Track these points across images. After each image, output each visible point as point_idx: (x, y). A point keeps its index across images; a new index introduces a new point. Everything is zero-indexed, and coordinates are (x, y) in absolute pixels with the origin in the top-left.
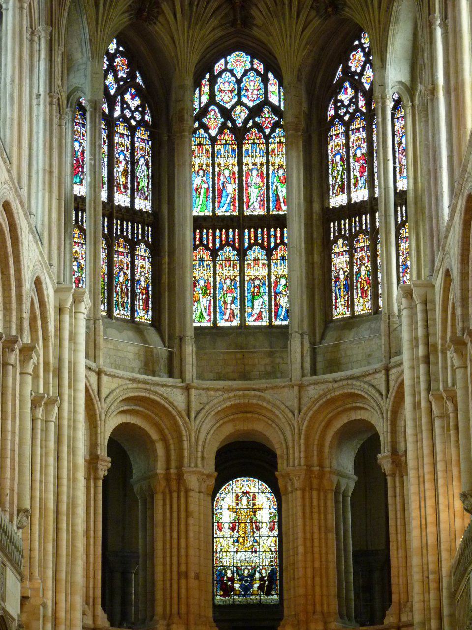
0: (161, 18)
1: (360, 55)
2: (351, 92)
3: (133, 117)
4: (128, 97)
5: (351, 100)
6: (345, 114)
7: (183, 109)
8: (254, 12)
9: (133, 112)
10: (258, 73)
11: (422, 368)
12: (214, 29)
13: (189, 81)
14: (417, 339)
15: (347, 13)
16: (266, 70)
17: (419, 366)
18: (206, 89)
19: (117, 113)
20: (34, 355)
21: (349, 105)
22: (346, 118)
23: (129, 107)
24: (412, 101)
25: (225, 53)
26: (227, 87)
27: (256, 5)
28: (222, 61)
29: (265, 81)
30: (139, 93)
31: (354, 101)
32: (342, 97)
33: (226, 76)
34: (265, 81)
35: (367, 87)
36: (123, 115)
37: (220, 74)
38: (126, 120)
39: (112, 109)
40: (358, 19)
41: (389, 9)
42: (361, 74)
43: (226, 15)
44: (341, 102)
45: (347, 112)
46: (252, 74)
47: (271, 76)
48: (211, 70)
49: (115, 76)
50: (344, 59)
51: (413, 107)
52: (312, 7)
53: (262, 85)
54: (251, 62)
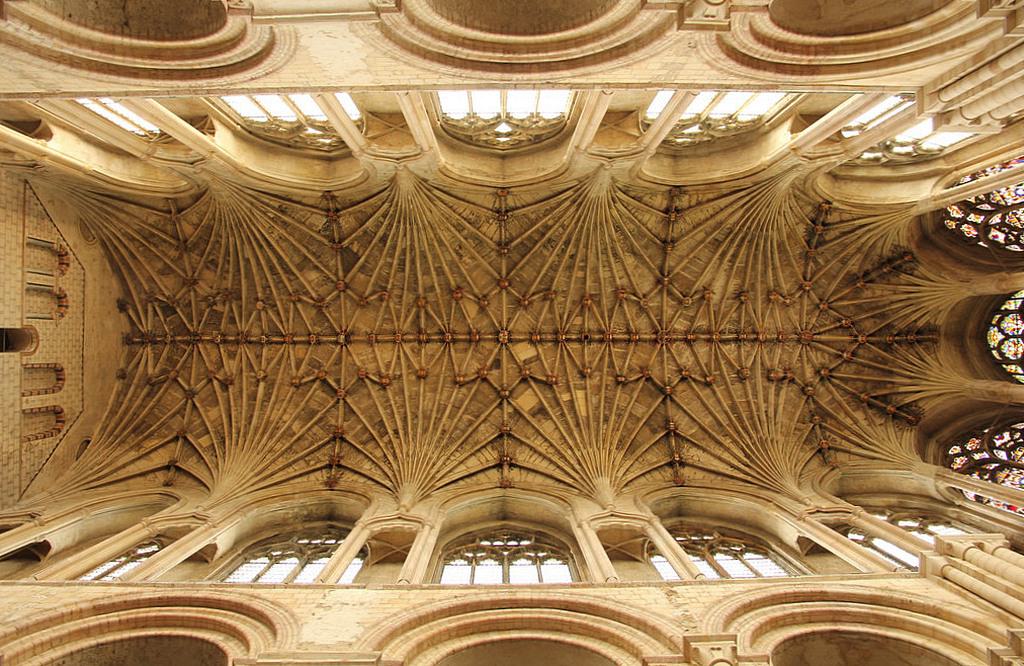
0: (920, 404)
1: (964, 227)
2: (994, 232)
3: (1015, 441)
4: (998, 443)
5: (999, 230)
6: (1013, 235)
7: (988, 392)
8: (920, 324)
9: (1012, 440)
10: (1001, 319)
11: (1005, 65)
12: (937, 360)
13: (997, 386)
14: (984, 85)
15: (904, 243)
16: (997, 310)
17: (1012, 70)
18: (1013, 367)
19: (1002, 455)
20: (694, 645)
21: (1003, 232)
22: (1016, 233)
23: (1005, 444)
24: (950, 172)
25: (989, 350)
26: (1013, 349)
27: (915, 321)
28: (994, 352)
29: (1008, 312)
30: (999, 432)
31: (1000, 227)
32: (1001, 238)
33: (1005, 348)
34: (1008, 312)
35: (983, 217)
36: (1008, 451)
37: (1002, 354)
38: (1013, 448)
39: (996, 460)
40: (904, 233)
41: (872, 207)
42: (974, 224)
43: (927, 349)
44: (1006, 239)
45: (1009, 233)
46: (1004, 325)
47: (1003, 308)
48: (998, 364)
49: (977, 451)
50: (971, 243)
51: (957, 169)
52: (911, 275)
53: (1011, 316)
54: (994, 326)
